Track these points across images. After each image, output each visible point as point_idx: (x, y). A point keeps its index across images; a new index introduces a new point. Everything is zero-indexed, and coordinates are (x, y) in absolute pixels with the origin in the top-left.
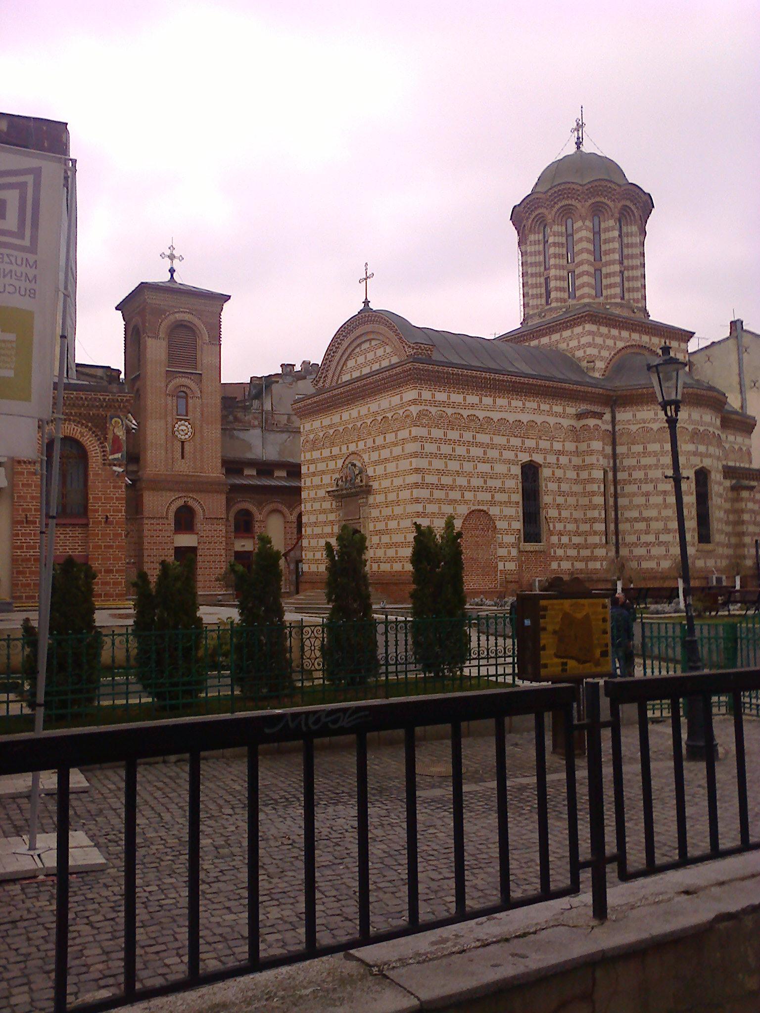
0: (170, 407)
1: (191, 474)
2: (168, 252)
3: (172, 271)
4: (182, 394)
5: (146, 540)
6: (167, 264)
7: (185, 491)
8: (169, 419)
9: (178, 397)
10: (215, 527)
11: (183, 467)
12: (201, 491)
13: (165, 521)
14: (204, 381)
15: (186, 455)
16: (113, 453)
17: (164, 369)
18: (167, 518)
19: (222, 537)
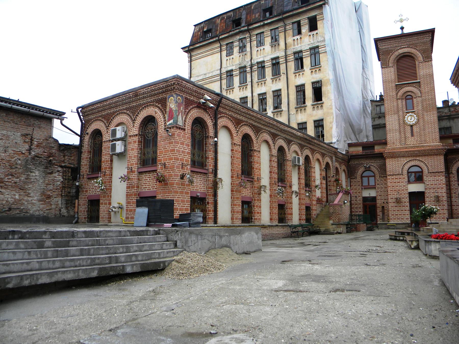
0: (400, 106)
1: (417, 145)
2: (398, 19)
3: (402, 28)
4: (408, 97)
5: (389, 189)
6: (400, 25)
7: (414, 156)
8: (401, 113)
9: (406, 99)
10: (437, 178)
11: (412, 142)
12: (425, 156)
13: (401, 176)
14: (422, 86)
15: (415, 134)
16: (169, 120)
17: (394, 85)
18: (402, 175)
19: (443, 184)
